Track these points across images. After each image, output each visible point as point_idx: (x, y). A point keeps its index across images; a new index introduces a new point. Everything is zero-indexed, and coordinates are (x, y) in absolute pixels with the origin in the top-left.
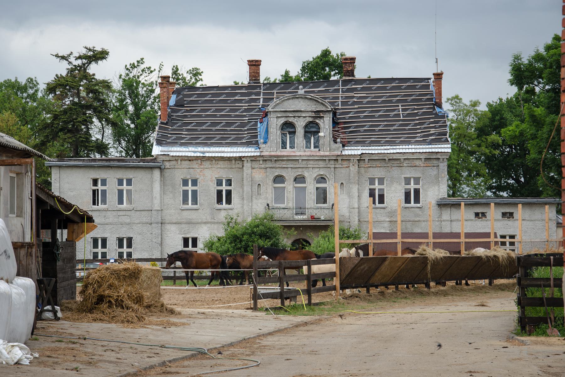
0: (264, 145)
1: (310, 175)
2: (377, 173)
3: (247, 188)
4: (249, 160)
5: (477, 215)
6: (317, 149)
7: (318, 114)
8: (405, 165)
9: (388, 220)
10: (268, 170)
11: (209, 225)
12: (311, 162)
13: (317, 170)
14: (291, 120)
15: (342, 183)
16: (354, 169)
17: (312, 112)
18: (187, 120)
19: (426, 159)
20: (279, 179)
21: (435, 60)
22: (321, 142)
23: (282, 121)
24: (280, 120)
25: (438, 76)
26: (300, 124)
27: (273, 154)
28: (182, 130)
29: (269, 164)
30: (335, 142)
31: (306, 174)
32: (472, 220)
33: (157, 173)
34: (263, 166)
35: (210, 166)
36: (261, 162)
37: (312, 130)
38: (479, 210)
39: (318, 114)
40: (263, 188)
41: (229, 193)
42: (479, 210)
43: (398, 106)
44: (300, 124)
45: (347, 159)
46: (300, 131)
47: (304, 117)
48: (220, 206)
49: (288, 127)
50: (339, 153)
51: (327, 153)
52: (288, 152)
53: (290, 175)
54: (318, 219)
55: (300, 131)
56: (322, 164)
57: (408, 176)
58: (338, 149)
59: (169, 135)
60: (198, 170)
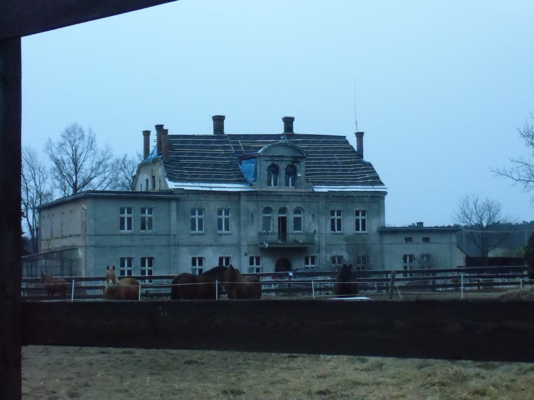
0: (255, 183)
1: (291, 207)
2: (338, 207)
3: (243, 218)
4: (245, 194)
5: (406, 239)
6: (294, 187)
7: (296, 160)
8: (356, 200)
9: (345, 243)
10: (260, 202)
11: (213, 247)
12: (292, 197)
13: (295, 203)
14: (276, 163)
15: (313, 215)
16: (322, 203)
17: (291, 157)
18: (183, 161)
19: (372, 197)
20: (268, 210)
21: (355, 123)
22: (298, 181)
23: (269, 163)
24: (268, 162)
25: (360, 136)
26: (283, 166)
27: (263, 189)
28: (182, 169)
29: (260, 198)
30: (308, 182)
31: (288, 207)
32: (402, 243)
33: (174, 205)
34: (255, 199)
35: (214, 199)
36: (254, 197)
37: (292, 172)
38: (408, 236)
39: (296, 160)
40: (255, 218)
41: (227, 221)
42: (408, 236)
43: (334, 156)
44: (283, 166)
45: (319, 194)
46: (282, 173)
47: (286, 161)
48: (193, 232)
49: (274, 170)
50: (311, 190)
51: (303, 190)
52: (272, 188)
53: (276, 207)
54: (298, 243)
55: (282, 173)
56: (299, 199)
57: (357, 209)
58: (310, 187)
59: (174, 173)
60: (204, 202)
